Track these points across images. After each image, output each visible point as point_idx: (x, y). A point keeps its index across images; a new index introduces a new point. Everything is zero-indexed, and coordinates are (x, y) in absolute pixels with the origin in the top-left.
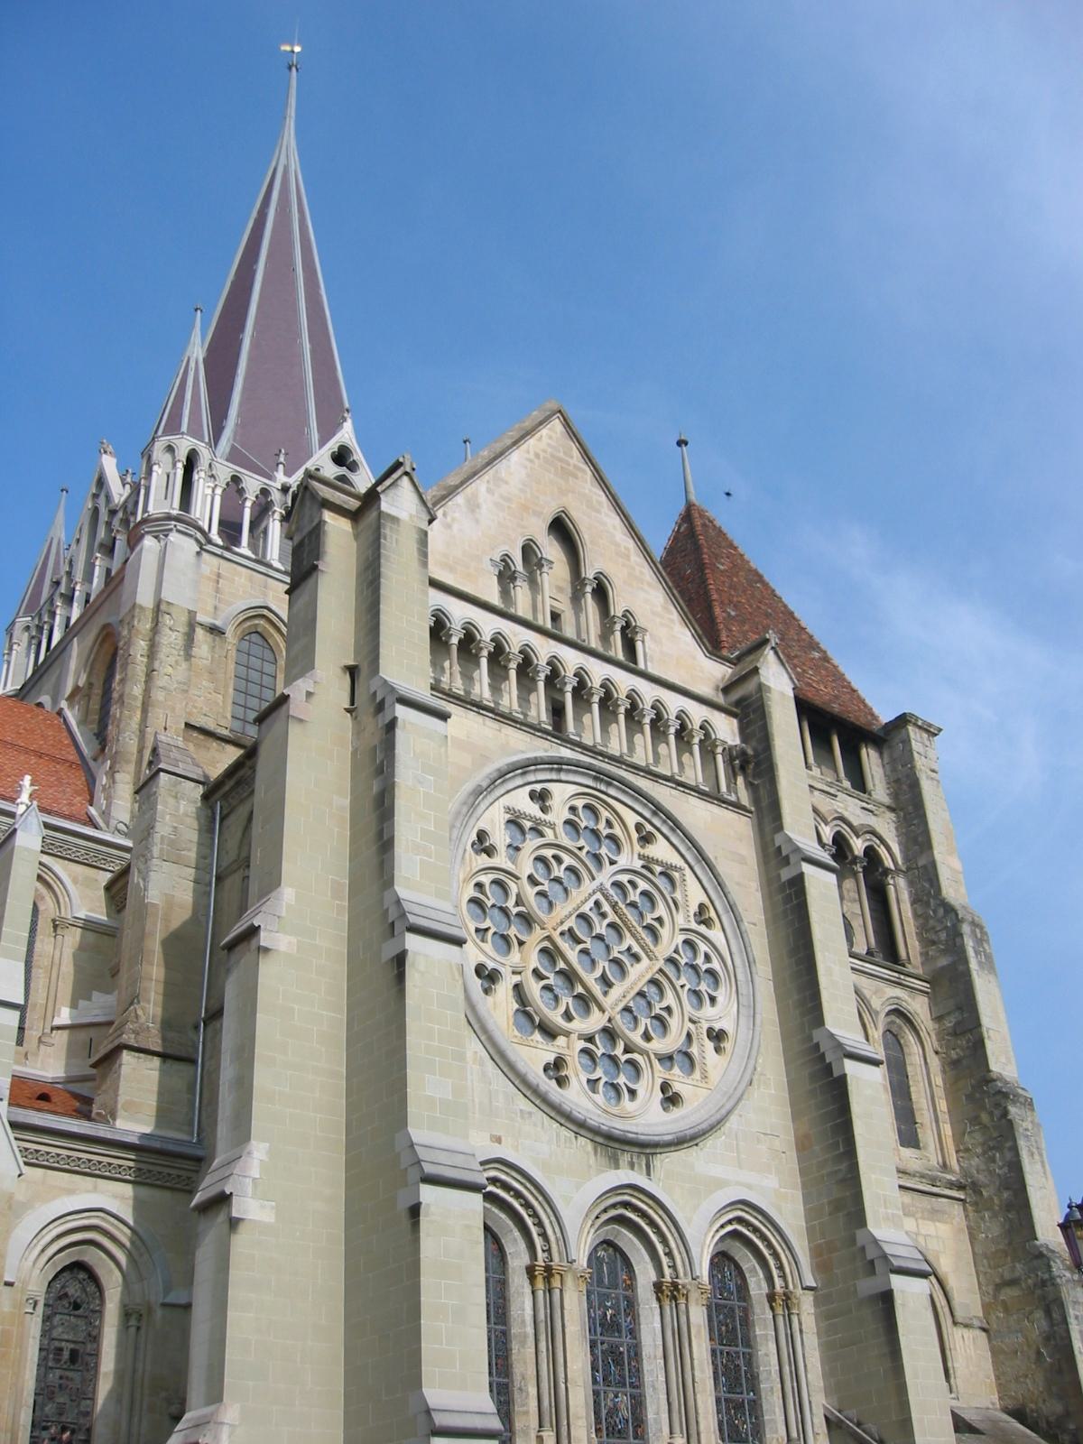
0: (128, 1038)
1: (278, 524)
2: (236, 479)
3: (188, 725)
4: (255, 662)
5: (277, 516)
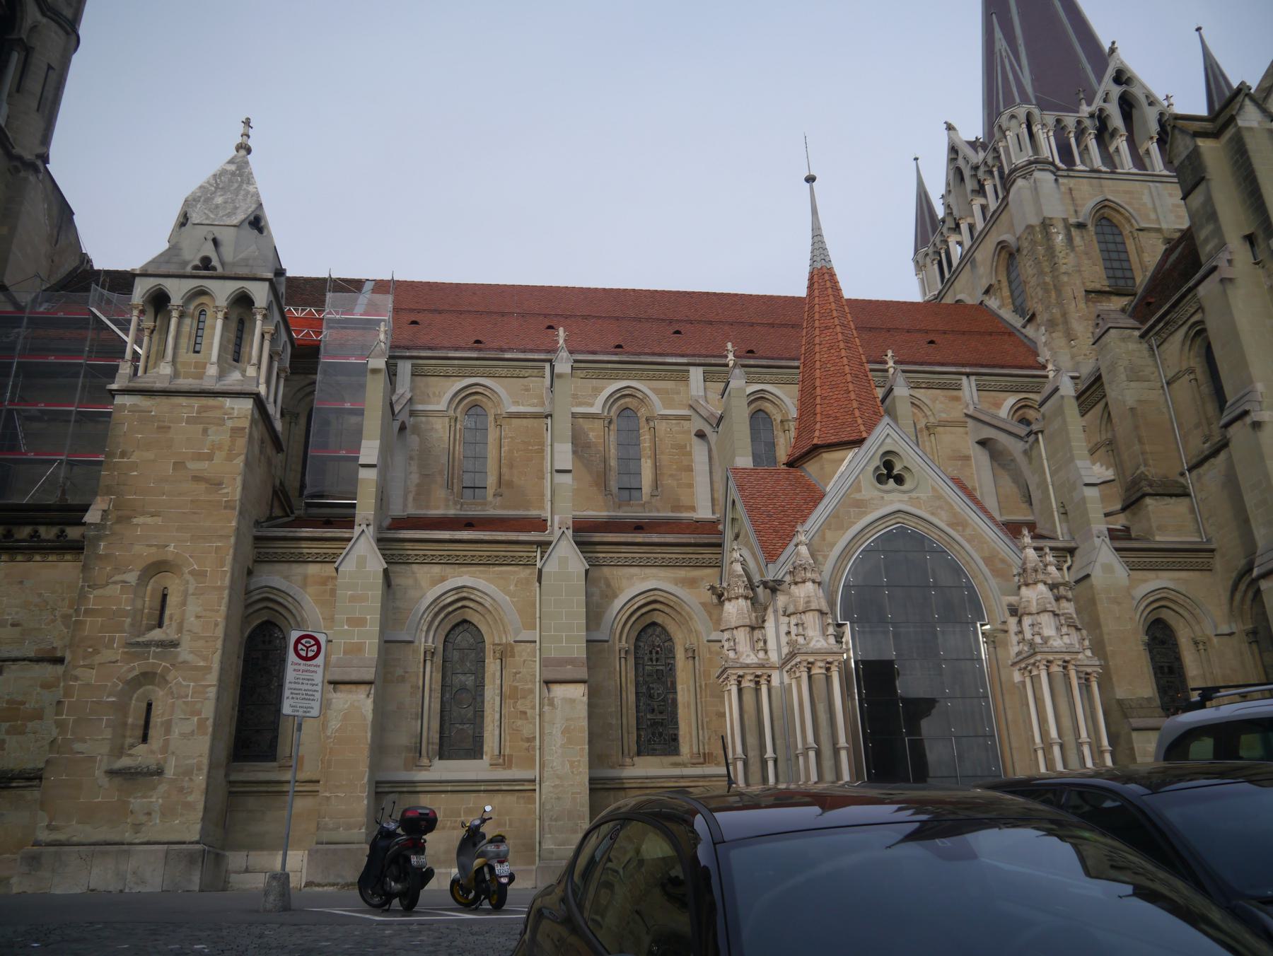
0: (1148, 490)
1: (1094, 141)
2: (1058, 121)
3: (1088, 292)
4: (1110, 238)
5: (1092, 136)
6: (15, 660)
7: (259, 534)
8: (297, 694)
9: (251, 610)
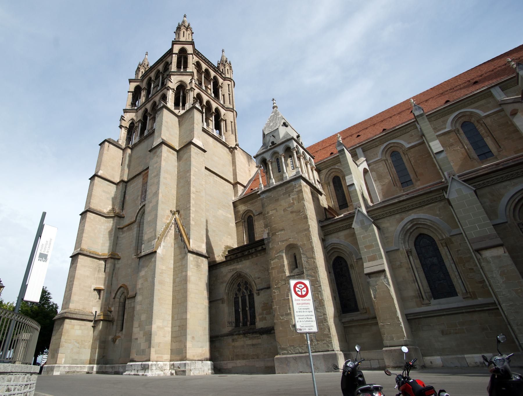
6: (262, 289)
7: (322, 225)
8: (302, 319)
9: (330, 254)
